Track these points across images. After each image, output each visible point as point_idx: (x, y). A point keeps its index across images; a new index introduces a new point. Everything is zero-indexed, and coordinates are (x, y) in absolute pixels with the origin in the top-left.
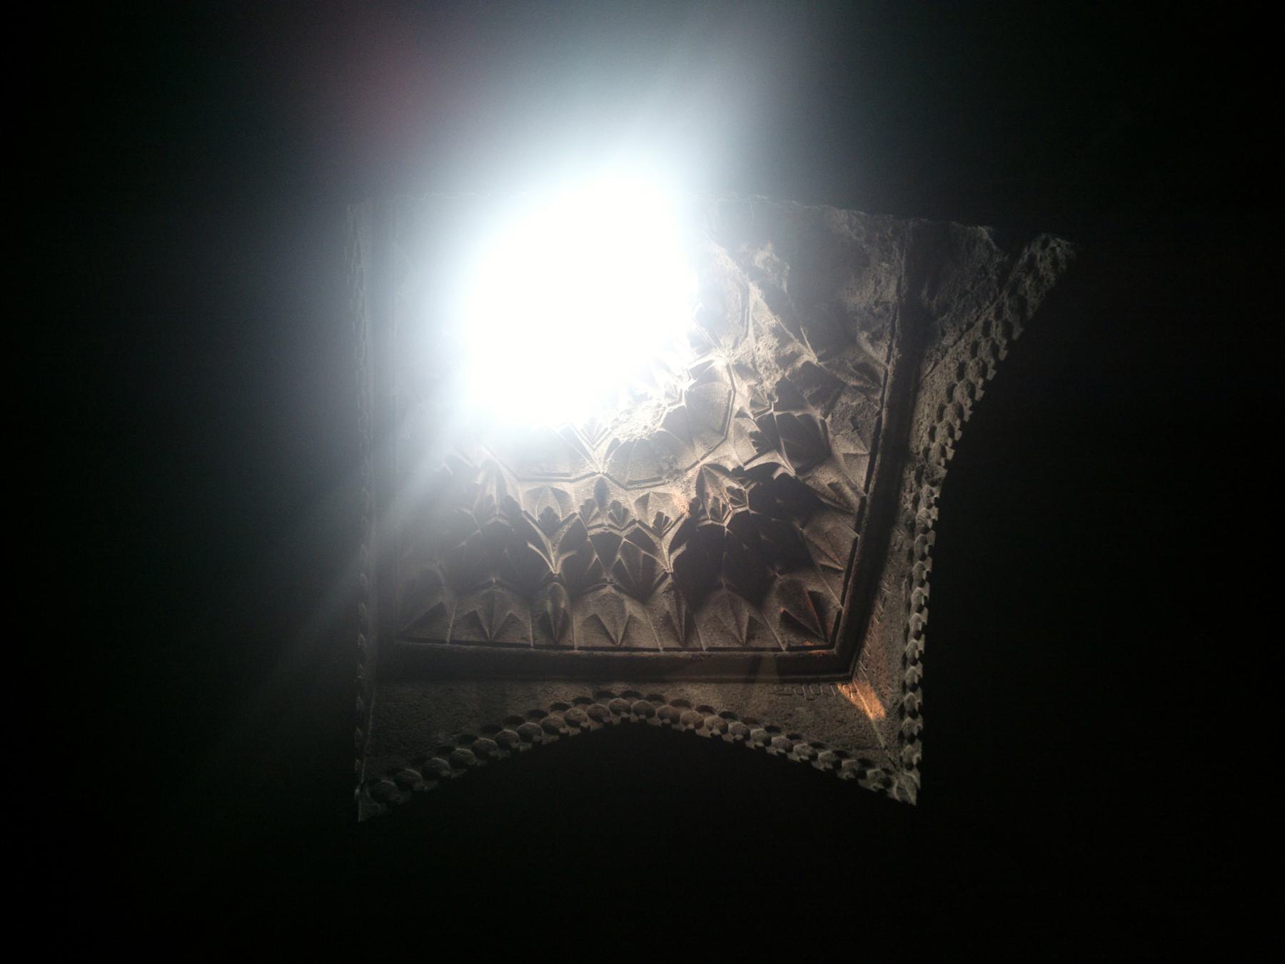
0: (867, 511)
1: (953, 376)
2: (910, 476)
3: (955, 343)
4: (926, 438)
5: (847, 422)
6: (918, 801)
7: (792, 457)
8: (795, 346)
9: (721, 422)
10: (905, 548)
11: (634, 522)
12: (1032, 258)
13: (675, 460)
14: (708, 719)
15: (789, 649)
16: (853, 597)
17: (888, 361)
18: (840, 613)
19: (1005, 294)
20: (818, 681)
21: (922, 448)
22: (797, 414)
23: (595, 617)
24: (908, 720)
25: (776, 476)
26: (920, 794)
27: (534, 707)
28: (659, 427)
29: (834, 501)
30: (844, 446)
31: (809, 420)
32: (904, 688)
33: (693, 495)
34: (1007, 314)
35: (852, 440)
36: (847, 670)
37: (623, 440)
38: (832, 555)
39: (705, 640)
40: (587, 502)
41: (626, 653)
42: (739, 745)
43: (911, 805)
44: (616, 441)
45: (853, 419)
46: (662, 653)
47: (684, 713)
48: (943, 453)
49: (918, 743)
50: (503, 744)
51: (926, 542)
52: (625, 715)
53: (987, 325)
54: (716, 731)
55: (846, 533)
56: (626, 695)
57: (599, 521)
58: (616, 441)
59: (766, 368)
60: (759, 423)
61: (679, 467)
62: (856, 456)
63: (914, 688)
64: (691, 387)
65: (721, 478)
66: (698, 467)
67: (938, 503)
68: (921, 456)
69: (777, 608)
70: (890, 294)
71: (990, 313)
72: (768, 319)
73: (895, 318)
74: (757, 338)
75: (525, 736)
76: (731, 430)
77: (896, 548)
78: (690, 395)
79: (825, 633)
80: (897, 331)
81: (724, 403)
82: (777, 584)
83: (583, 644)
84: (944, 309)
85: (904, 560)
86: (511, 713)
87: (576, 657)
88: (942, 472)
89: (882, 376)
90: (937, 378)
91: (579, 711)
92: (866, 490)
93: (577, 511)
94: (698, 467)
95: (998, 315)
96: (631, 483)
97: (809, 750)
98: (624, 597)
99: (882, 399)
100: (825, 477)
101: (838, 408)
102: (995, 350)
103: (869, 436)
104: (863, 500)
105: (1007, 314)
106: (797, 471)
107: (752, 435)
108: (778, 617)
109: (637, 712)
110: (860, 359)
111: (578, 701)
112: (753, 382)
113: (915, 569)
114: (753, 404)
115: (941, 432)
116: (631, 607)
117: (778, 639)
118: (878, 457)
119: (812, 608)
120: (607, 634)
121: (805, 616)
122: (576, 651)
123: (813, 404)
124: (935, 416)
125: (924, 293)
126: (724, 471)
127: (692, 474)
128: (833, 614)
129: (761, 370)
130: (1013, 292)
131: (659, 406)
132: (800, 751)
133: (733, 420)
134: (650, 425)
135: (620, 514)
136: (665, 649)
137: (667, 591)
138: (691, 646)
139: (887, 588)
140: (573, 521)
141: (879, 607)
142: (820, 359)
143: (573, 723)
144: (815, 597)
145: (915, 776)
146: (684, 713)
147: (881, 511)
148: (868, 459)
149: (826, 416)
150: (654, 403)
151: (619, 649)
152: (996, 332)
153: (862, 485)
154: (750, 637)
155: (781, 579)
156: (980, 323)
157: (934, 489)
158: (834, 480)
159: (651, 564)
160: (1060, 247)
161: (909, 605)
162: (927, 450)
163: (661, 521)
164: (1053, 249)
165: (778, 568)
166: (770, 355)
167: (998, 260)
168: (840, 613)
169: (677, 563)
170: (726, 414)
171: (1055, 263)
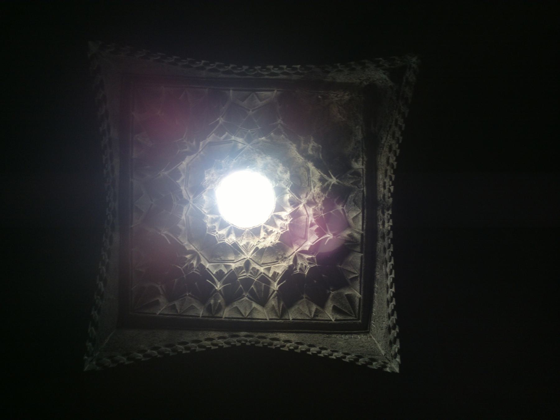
6: (400, 370)
9: (304, 233)
11: (261, 273)
13: (285, 254)
15: (336, 320)
20: (351, 334)
21: (382, 196)
24: (393, 331)
26: (400, 366)
28: (277, 241)
35: (355, 210)
37: (260, 248)
39: (291, 316)
41: (249, 320)
43: (397, 373)
57: (245, 274)
58: (257, 248)
61: (286, 256)
66: (294, 254)
69: (330, 305)
72: (316, 173)
79: (355, 312)
82: (331, 296)
83: (227, 316)
89: (361, 173)
94: (294, 254)
96: (263, 264)
99: (363, 183)
104: (362, 235)
108: (331, 308)
109: (250, 342)
112: (314, 207)
117: (329, 315)
122: (223, 319)
127: (292, 257)
134: (273, 241)
136: (270, 319)
138: (284, 318)
148: (361, 214)
151: (245, 318)
154: (315, 316)
159: (267, 289)
165: (331, 289)
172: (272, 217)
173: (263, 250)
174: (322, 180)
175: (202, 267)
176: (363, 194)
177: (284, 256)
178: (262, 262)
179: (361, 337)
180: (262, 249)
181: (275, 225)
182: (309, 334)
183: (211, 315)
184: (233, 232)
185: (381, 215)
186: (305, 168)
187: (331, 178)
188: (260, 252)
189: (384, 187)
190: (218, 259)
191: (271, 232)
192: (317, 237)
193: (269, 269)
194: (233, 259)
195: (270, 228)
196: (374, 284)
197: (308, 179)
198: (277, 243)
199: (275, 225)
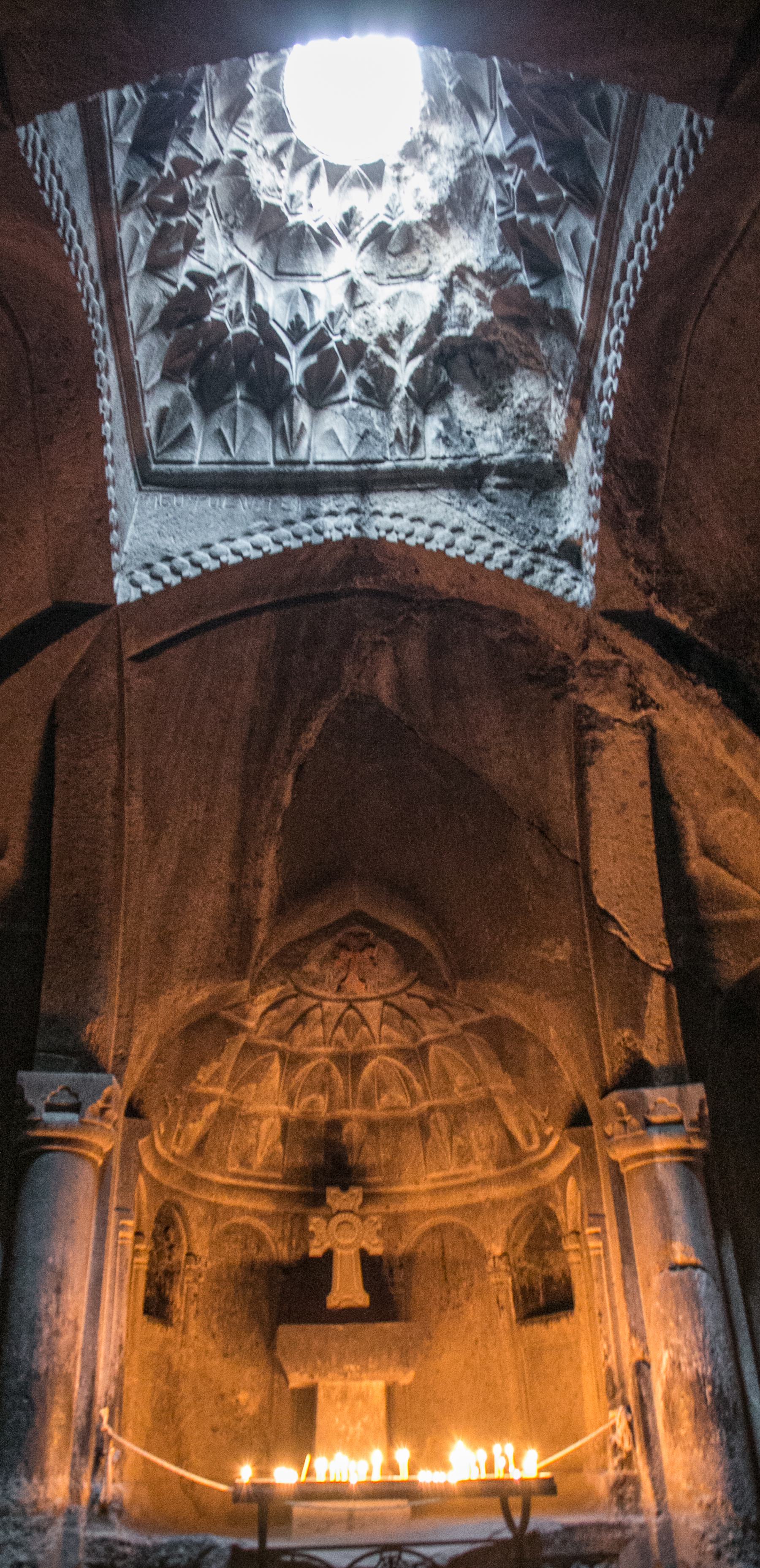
3: (474, 519)
4: (389, 510)
9: (287, 270)
10: (292, 516)
12: (561, 571)
13: (238, 228)
15: (148, 429)
17: (433, 458)
18: (191, 462)
21: (378, 508)
22: (341, 367)
25: (279, 358)
28: (263, 198)
29: (291, 431)
31: (341, 383)
33: (225, 269)
34: (518, 562)
37: (245, 162)
38: (239, 440)
45: (367, 432)
48: (389, 531)
49: (159, 587)
51: (310, 534)
55: (262, 450)
59: (367, 322)
64: (310, 227)
65: (243, 290)
66: (243, 259)
67: (346, 537)
68: (372, 509)
70: (485, 447)
73: (469, 457)
74: (388, 302)
76: (286, 286)
77: (283, 505)
78: (301, 228)
79: (166, 450)
81: (306, 269)
84: (492, 500)
85: (281, 516)
90: (439, 506)
92: (316, 463)
95: (513, 553)
99: (399, 460)
101: (366, 410)
103: (362, 454)
104: (306, 463)
105: (518, 562)
106: (299, 388)
107: (298, 317)
110: (420, 428)
112: (347, 307)
113: (284, 532)
115: (402, 524)
118: (350, 468)
119: (178, 430)
123: (357, 382)
124: (412, 515)
126: (251, 293)
127: (238, 258)
128: (183, 454)
129: (359, 315)
130: (535, 561)
131: (280, 190)
137: (165, 294)
139: (246, 505)
141: (224, 502)
145: (135, 595)
147: (312, 484)
148: (343, 458)
149: (354, 400)
150: (281, 184)
152: (501, 555)
153: (319, 458)
154: (148, 392)
155: (185, 389)
156: (499, 538)
157: (353, 529)
158: (307, 426)
162: (378, 513)
167: (551, 542)
168: (191, 462)
170: (297, 275)
171: (568, 591)
172: (314, 156)
174: (402, 331)
176: (380, 462)
177: (234, 231)
180: (244, 168)
185: (346, 507)
186: (426, 270)
187: (409, 360)
188: (237, 170)
189: (394, 515)
191: (281, 166)
192: (286, 325)
194: (217, 114)
195: (287, 160)
197: (403, 277)
198: (258, 201)
199: (296, 168)
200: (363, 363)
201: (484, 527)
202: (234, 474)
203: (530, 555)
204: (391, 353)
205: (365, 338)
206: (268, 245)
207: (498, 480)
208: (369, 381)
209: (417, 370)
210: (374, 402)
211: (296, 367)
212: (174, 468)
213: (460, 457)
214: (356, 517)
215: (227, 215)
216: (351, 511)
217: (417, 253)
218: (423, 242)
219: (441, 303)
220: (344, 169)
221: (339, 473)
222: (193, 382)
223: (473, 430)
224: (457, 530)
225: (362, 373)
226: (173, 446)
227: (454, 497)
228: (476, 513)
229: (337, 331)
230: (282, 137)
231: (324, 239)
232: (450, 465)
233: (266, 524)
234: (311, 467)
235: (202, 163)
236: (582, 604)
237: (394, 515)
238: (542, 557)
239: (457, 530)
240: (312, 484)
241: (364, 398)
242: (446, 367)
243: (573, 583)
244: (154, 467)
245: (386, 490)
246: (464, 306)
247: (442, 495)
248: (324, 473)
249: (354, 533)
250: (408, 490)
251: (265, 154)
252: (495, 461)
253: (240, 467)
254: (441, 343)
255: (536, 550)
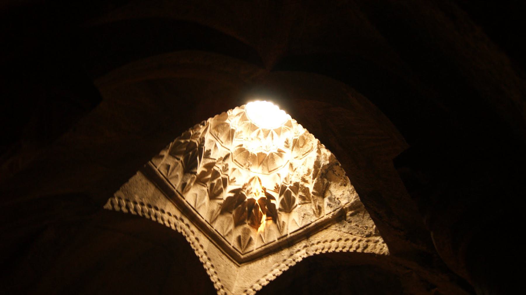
0: (285, 238)
1: (336, 239)
2: (303, 243)
4: (316, 242)
5: (303, 213)
7: (282, 203)
8: (309, 178)
9: (272, 169)
10: (285, 257)
11: (227, 175)
12: (378, 241)
14: (201, 250)
16: (260, 252)
18: (253, 251)
19: (366, 239)
21: (313, 242)
23: (196, 195)
25: (272, 201)
27: (163, 208)
30: (295, 215)
31: (294, 200)
32: (252, 287)
33: (247, 182)
34: (361, 244)
36: (240, 263)
37: (243, 147)
39: (217, 227)
40: (221, 158)
42: (202, 264)
44: (241, 145)
45: (305, 214)
46: (204, 221)
47: (196, 243)
48: (316, 250)
50: (149, 214)
51: (291, 263)
52: (183, 231)
53: (354, 240)
54: (200, 256)
56: (188, 225)
60: (282, 186)
62: (296, 223)
63: (254, 290)
68: (311, 243)
69: (239, 232)
70: (343, 202)
71: (359, 238)
75: (156, 216)
77: (283, 254)
80: (336, 212)
84: (350, 222)
85: (282, 259)
86: (157, 205)
87: (183, 203)
88: (311, 254)
91: (173, 220)
92: (290, 234)
93: (217, 159)
95: (360, 241)
96: (235, 160)
97: (216, 280)
98: (207, 194)
100: (283, 217)
101: (304, 206)
102: (351, 247)
103: (304, 224)
105: (361, 244)
106: (280, 210)
108: (238, 235)
110: (321, 205)
111: (176, 217)
114: (286, 179)
115: (320, 246)
116: (206, 199)
117: (232, 242)
120: (196, 203)
121: (244, 241)
122: (185, 201)
124: (324, 240)
125: (350, 212)
128: (250, 248)
132: (214, 278)
133: (274, 174)
135: (225, 169)
139: (271, 259)
140: (213, 161)
141: (264, 260)
142: (313, 193)
143: (169, 223)
144: (251, 239)
146: (196, 243)
149: (299, 204)
154: (227, 235)
156: (354, 237)
158: (285, 221)
160: (386, 249)
161: (272, 270)
162: (313, 244)
163: (233, 180)
164: (384, 246)
166: (302, 175)
169: (229, 198)
172: (269, 131)
173: (244, 149)
175: (203, 140)
178: (235, 158)
179: (234, 267)
181: (266, 135)
182: (214, 246)
183: (181, 193)
184: (241, 115)
185: (302, 247)
188: (241, 150)
189: (319, 242)
190: (216, 133)
192: (273, 189)
193: (234, 169)
194: (223, 142)
196: (265, 257)
198: (254, 155)
200: (300, 189)
201: (348, 234)
202: (266, 249)
203: (366, 239)
204: (306, 182)
205: (298, 181)
206: (264, 165)
207: (350, 212)
208: (303, 195)
209: (315, 184)
210: (307, 201)
211: (277, 203)
212: (248, 255)
213: (335, 210)
214: (306, 249)
215: (245, 164)
216: (306, 246)
217: (308, 143)
218: (308, 138)
219: (318, 157)
220: (280, 129)
221: (298, 234)
222: (249, 222)
223: (339, 197)
224: (339, 240)
225: (300, 193)
226: (247, 247)
227: (337, 227)
228: (344, 230)
229: (289, 182)
230: (257, 131)
231: (280, 153)
232: (333, 215)
233: (277, 264)
234: (289, 236)
235: (216, 161)
236: (386, 254)
237: (319, 242)
238: (370, 238)
239: (339, 240)
240: (288, 243)
241: (303, 202)
242: (326, 178)
243: (383, 245)
244: (242, 257)
245: (315, 234)
246: (324, 154)
247: (333, 227)
248: (293, 236)
249: (305, 256)
250: (321, 231)
251: (252, 139)
252: (347, 206)
253: (267, 246)
254: (321, 170)
255: (368, 236)
